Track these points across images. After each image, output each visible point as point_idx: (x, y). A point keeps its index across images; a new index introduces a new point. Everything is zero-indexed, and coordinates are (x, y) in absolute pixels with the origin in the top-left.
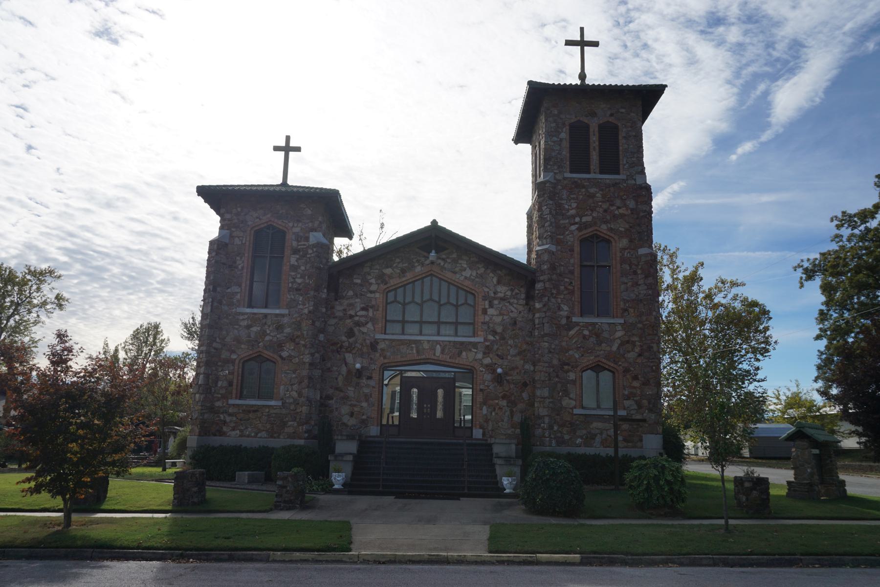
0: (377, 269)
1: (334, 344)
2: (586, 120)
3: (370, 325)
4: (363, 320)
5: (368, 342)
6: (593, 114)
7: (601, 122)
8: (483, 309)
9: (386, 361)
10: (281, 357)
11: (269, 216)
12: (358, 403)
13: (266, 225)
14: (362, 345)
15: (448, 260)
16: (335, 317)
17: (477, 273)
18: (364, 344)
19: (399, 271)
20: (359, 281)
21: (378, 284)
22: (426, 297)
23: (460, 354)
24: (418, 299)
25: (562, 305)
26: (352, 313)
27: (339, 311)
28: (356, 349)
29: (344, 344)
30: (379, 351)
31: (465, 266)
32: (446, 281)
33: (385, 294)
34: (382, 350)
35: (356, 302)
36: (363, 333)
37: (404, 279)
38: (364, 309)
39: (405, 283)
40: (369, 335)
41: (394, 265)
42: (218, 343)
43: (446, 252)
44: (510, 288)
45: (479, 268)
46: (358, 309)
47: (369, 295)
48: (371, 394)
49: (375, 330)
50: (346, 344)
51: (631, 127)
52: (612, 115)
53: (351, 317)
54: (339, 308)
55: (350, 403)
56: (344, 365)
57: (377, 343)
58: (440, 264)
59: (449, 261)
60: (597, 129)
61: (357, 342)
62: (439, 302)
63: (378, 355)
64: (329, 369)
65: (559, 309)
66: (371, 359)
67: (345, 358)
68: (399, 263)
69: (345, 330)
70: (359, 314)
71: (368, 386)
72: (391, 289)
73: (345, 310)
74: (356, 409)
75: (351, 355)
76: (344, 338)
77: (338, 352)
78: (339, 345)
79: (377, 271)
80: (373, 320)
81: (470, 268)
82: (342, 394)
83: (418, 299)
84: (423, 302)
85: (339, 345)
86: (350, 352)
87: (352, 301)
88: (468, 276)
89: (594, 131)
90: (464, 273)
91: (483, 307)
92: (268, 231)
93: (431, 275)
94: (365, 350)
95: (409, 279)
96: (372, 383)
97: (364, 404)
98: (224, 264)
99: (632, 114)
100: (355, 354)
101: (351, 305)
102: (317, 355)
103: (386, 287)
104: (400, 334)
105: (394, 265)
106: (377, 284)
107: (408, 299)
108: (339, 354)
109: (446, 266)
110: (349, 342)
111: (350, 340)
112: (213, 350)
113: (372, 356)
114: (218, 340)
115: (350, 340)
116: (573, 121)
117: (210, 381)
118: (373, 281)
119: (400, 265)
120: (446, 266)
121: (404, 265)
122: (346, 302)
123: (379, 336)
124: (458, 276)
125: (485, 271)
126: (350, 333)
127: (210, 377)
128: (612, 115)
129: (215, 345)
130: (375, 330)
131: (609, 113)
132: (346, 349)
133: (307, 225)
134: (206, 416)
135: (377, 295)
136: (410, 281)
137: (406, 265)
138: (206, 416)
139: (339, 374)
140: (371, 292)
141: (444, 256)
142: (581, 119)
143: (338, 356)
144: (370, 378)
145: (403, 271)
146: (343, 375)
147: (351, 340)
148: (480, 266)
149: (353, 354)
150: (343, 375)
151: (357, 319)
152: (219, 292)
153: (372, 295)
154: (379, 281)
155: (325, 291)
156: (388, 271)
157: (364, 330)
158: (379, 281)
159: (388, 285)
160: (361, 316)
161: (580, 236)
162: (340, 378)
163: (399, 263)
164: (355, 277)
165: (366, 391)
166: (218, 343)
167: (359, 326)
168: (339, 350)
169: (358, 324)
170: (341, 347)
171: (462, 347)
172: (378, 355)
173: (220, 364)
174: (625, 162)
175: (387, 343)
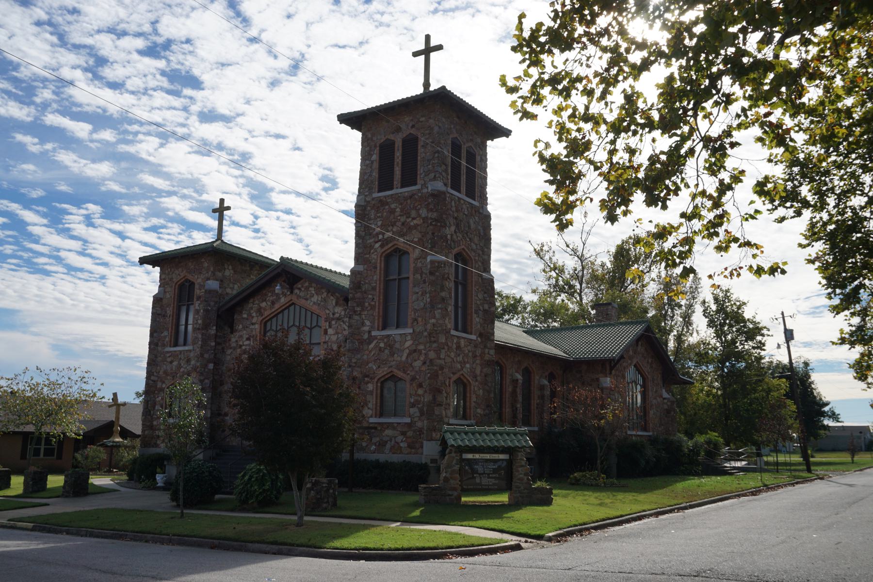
2: (391, 137)
6: (398, 130)
7: (404, 136)
16: (231, 348)
20: (245, 316)
21: (257, 316)
22: (291, 323)
24: (274, 328)
26: (241, 343)
37: (273, 310)
38: (248, 339)
45: (323, 293)
46: (245, 339)
52: (413, 126)
53: (241, 346)
54: (233, 340)
60: (401, 144)
81: (317, 294)
83: (274, 328)
87: (241, 333)
98: (159, 314)
101: (241, 336)
102: (206, 381)
103: (261, 318)
114: (155, 374)
116: (382, 141)
118: (254, 314)
119: (271, 298)
124: (309, 302)
128: (413, 126)
129: (152, 378)
131: (411, 125)
135: (257, 326)
136: (279, 310)
138: (146, 432)
140: (253, 324)
141: (300, 286)
145: (273, 303)
155: (215, 328)
156: (264, 304)
160: (246, 345)
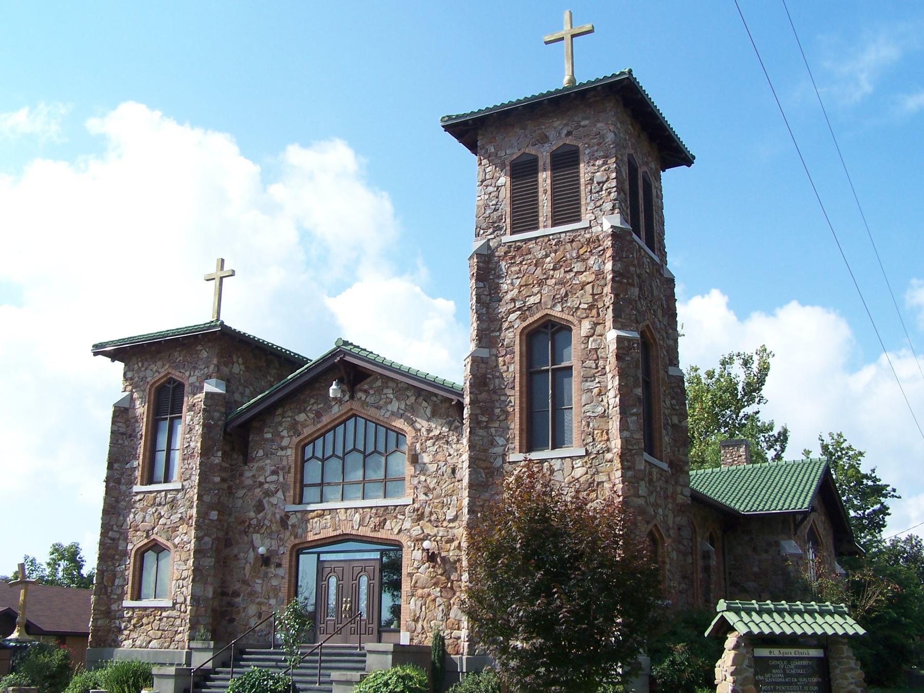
0: (289, 417)
1: (244, 522)
2: (532, 151)
3: (280, 494)
4: (273, 487)
5: (278, 516)
6: (544, 139)
7: (554, 148)
8: (413, 455)
9: (297, 541)
10: (174, 544)
11: (166, 367)
12: (265, 601)
13: (165, 379)
14: (271, 521)
15: (370, 391)
16: (243, 487)
17: (406, 404)
18: (273, 521)
19: (313, 416)
20: (269, 436)
21: (290, 436)
22: (350, 446)
23: (382, 524)
24: (319, 454)
25: (497, 438)
26: (262, 479)
27: (248, 478)
28: (265, 527)
29: (252, 522)
30: (290, 528)
31: (391, 396)
32: (374, 422)
33: (300, 449)
34: (294, 526)
35: (266, 465)
36: (273, 505)
37: (319, 426)
38: (274, 473)
39: (323, 431)
40: (279, 507)
41: (308, 408)
42: (116, 531)
43: (369, 380)
44: (448, 420)
45: (408, 397)
46: (268, 473)
47: (280, 453)
48: (280, 587)
49: (285, 500)
50: (254, 522)
51: (599, 144)
52: (569, 134)
53: (261, 484)
54: (248, 474)
55: (257, 600)
56: (251, 550)
57: (288, 517)
58: (361, 398)
59: (371, 392)
60: (548, 161)
61: (265, 518)
62: (364, 453)
63: (288, 533)
64: (236, 556)
65: (492, 444)
66: (281, 539)
67: (252, 540)
68: (313, 404)
69: (253, 504)
70: (268, 479)
71: (276, 576)
72: (306, 441)
73: (254, 476)
74: (264, 608)
75: (259, 535)
76: (252, 514)
77: (246, 532)
78: (247, 524)
79: (289, 419)
80: (284, 487)
81: (398, 399)
82: (249, 589)
83: (319, 454)
84: (345, 454)
85: (247, 524)
86: (258, 533)
87: (261, 464)
88: (395, 410)
89: (544, 165)
90: (390, 407)
91: (414, 453)
92: (169, 386)
93: (355, 416)
94: (274, 528)
95: (326, 425)
96: (281, 572)
97: (273, 602)
98: (123, 434)
99: (599, 125)
100: (263, 533)
101: (262, 469)
102: (207, 539)
103: (299, 439)
104: (318, 503)
105: (308, 408)
106: (289, 436)
107: (329, 453)
108: (247, 536)
109: (368, 400)
110: (258, 519)
111: (258, 516)
112: (109, 541)
113: (282, 536)
114: (115, 528)
115: (258, 516)
116: (515, 157)
117: (105, 579)
118: (285, 433)
119: (315, 407)
120: (368, 400)
121: (319, 406)
122: (256, 465)
123: (291, 508)
124: (383, 412)
125: (416, 400)
126: (260, 507)
127: (105, 574)
128: (569, 134)
129: (111, 534)
130: (285, 500)
131: (564, 132)
132: (254, 528)
133: (202, 372)
134: (100, 622)
135: (289, 452)
136: (329, 427)
137: (322, 405)
138: (100, 622)
139: (247, 562)
140: (282, 449)
141: (366, 387)
142: (527, 151)
143: (246, 538)
144: (279, 565)
145: (319, 415)
146: (250, 563)
147: (260, 516)
148: (409, 394)
149: (261, 534)
150: (250, 563)
151: (266, 486)
152: (117, 470)
153: (283, 453)
154: (291, 433)
155: (220, 454)
156: (302, 417)
157: (274, 500)
158: (291, 433)
159: (302, 437)
160: (272, 482)
161: (524, 328)
162: (248, 567)
163: (313, 404)
164: (265, 430)
165: (275, 582)
166: (116, 531)
167: (269, 496)
168: (247, 530)
169: (268, 494)
170: (250, 525)
171: (384, 513)
172: (288, 533)
173: (117, 557)
174: (588, 200)
175: (299, 515)
